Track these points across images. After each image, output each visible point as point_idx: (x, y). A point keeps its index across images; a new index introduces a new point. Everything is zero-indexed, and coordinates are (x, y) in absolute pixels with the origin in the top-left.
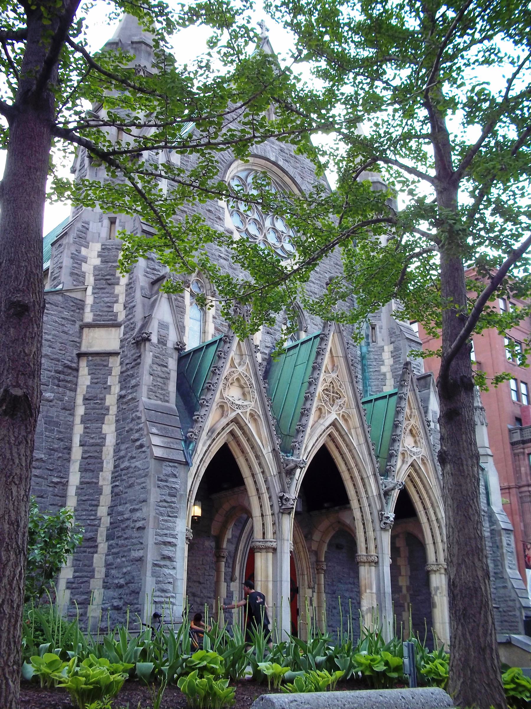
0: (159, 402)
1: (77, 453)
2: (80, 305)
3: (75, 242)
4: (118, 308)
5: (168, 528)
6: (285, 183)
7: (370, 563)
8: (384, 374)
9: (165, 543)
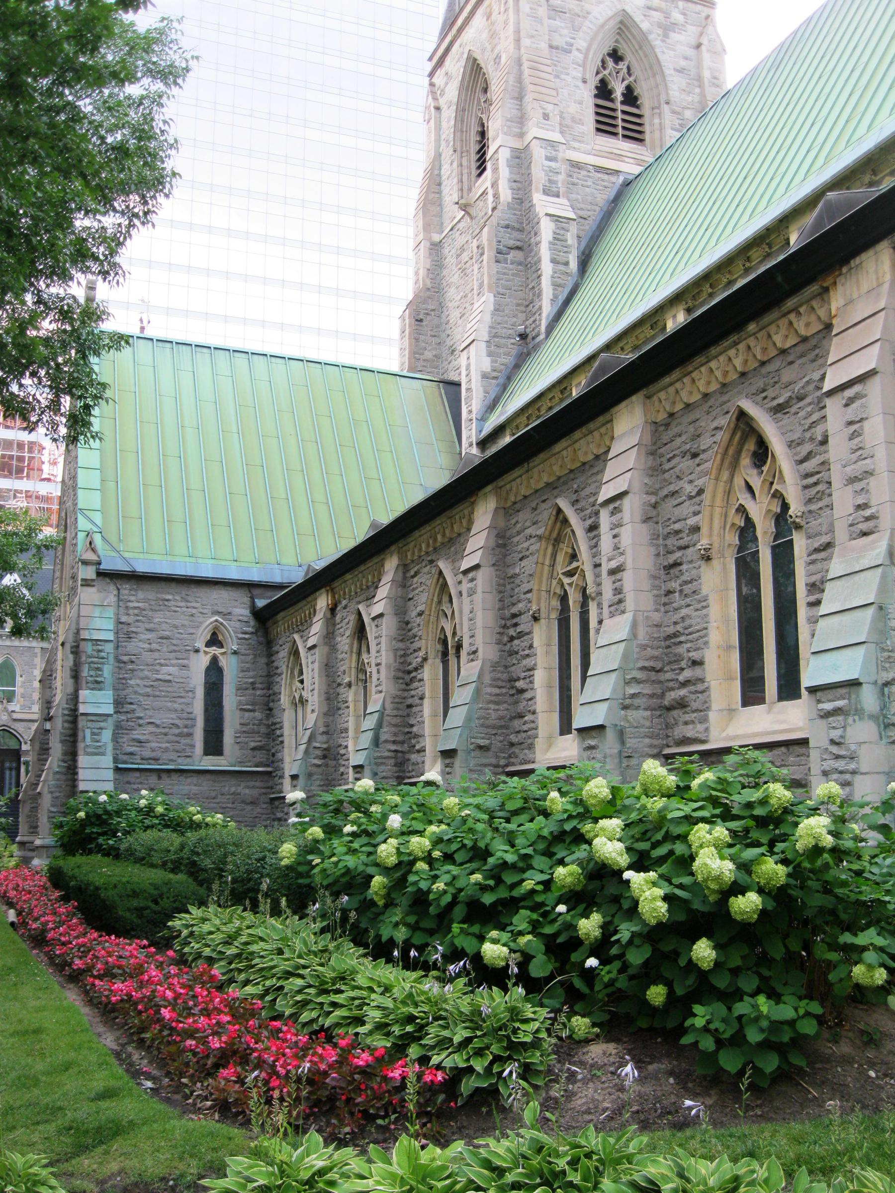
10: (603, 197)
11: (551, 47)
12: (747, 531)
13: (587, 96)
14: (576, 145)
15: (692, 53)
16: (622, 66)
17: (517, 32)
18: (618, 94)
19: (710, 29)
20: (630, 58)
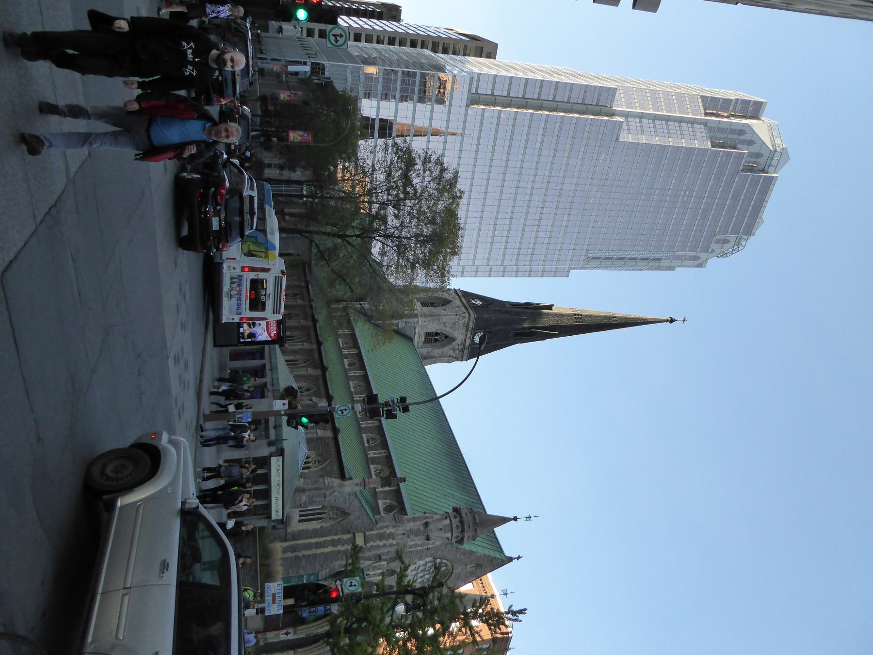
1: (321, 540)
2: (372, 530)
4: (372, 543)
6: (446, 576)
10: (408, 334)
11: (445, 323)
12: (297, 361)
13: (434, 330)
14: (421, 328)
15: (448, 355)
16: (444, 338)
17: (448, 315)
18: (436, 337)
19: (454, 359)
20: (446, 340)
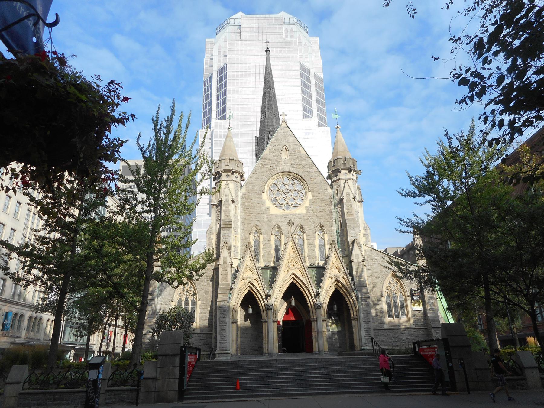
0: (225, 283)
3: (209, 235)
5: (223, 321)
7: (314, 321)
8: (345, 241)
9: (222, 325)
